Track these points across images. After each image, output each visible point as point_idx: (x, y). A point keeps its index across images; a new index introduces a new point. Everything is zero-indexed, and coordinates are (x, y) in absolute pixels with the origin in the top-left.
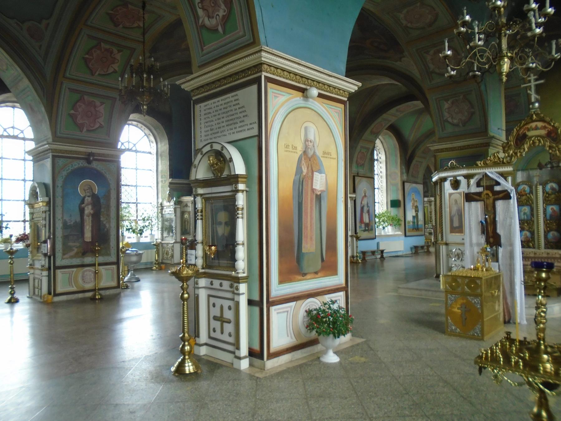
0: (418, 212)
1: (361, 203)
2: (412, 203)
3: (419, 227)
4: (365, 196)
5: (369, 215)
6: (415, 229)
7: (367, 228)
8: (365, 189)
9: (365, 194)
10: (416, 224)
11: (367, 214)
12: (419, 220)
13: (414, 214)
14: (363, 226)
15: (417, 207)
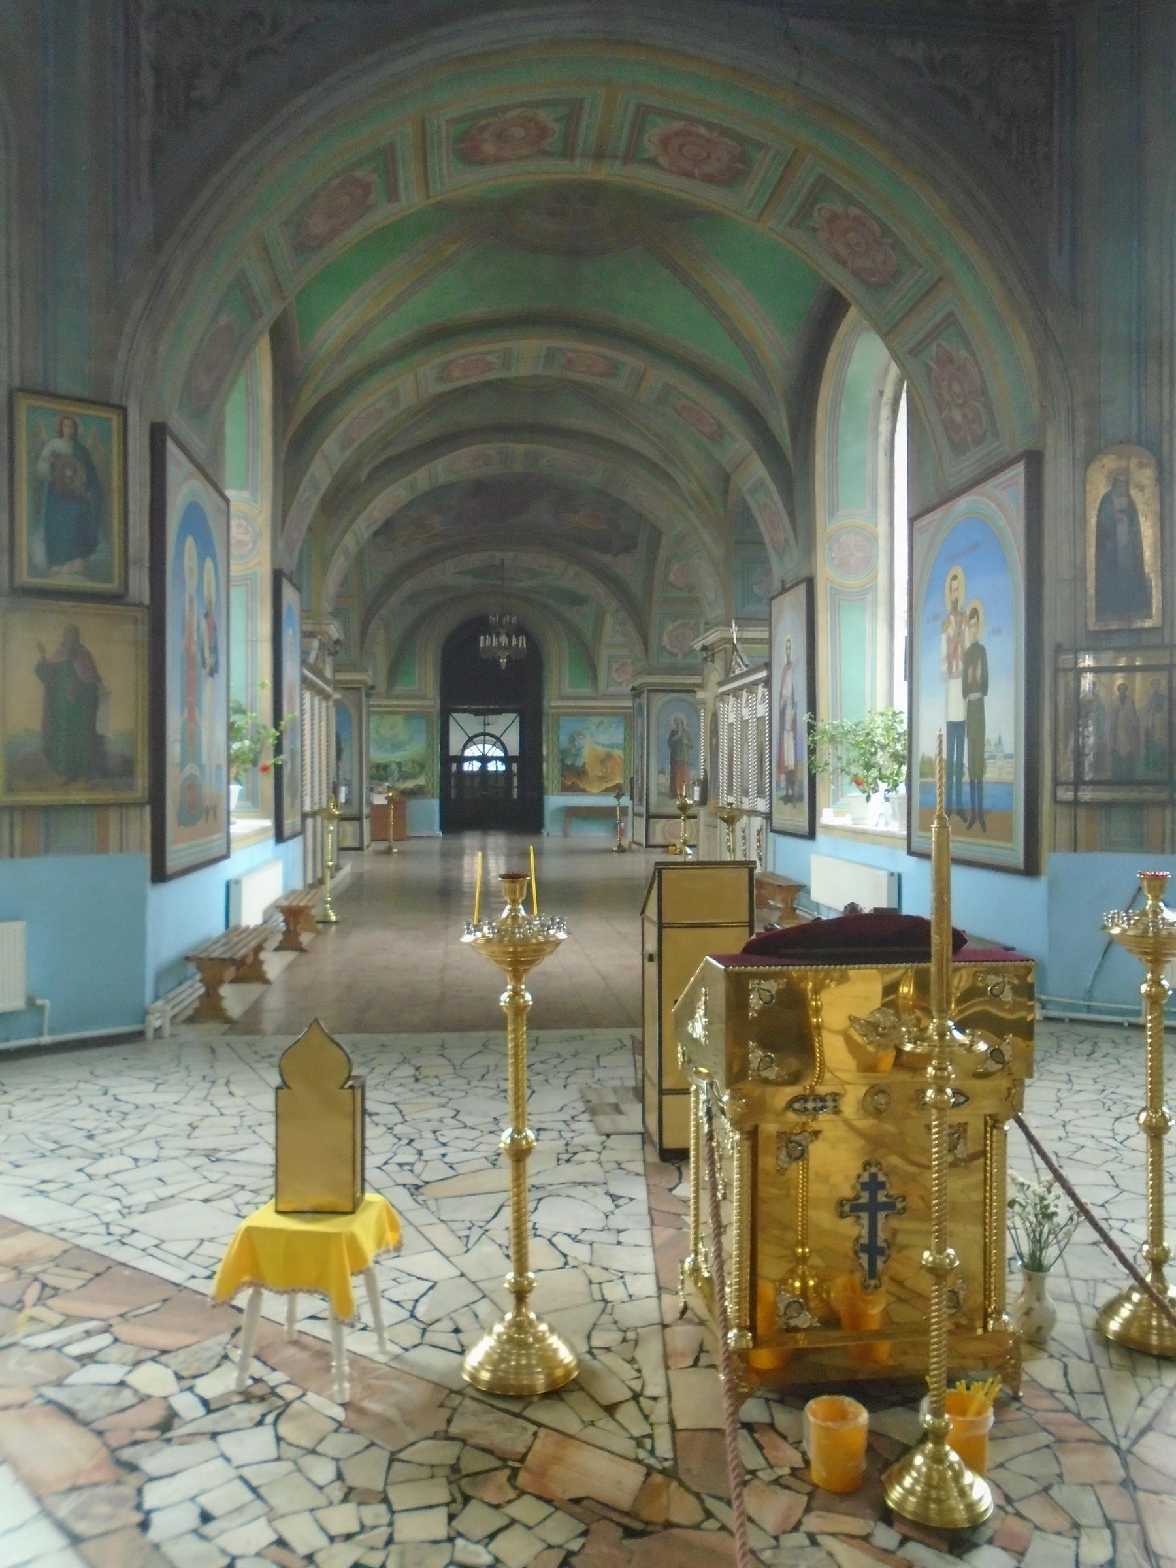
0: (983, 688)
1: (781, 697)
2: (949, 640)
3: (987, 803)
4: (789, 664)
5: (795, 738)
6: (961, 813)
7: (790, 792)
8: (789, 636)
9: (788, 656)
10: (966, 778)
11: (792, 734)
12: (989, 749)
13: (958, 713)
14: (783, 777)
15: (976, 654)
